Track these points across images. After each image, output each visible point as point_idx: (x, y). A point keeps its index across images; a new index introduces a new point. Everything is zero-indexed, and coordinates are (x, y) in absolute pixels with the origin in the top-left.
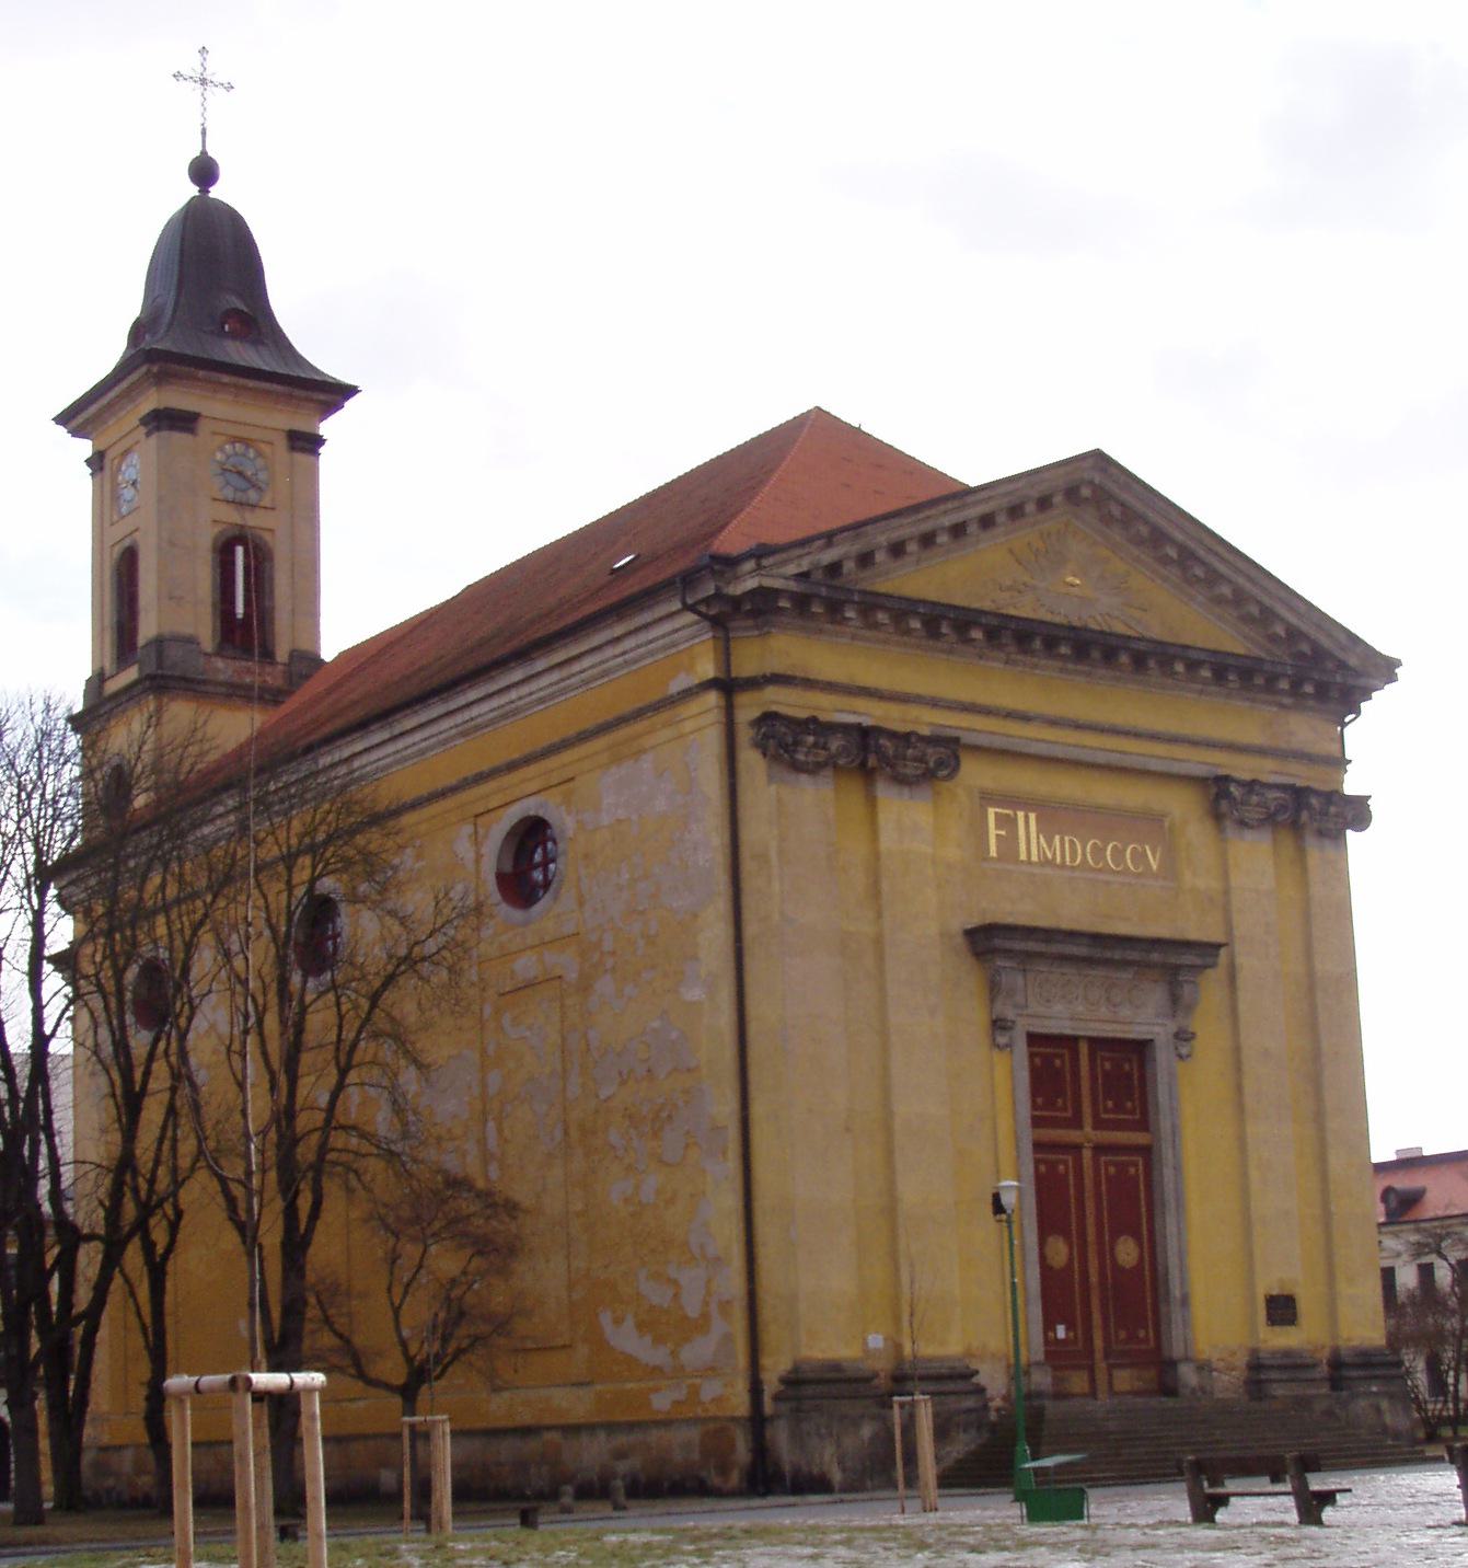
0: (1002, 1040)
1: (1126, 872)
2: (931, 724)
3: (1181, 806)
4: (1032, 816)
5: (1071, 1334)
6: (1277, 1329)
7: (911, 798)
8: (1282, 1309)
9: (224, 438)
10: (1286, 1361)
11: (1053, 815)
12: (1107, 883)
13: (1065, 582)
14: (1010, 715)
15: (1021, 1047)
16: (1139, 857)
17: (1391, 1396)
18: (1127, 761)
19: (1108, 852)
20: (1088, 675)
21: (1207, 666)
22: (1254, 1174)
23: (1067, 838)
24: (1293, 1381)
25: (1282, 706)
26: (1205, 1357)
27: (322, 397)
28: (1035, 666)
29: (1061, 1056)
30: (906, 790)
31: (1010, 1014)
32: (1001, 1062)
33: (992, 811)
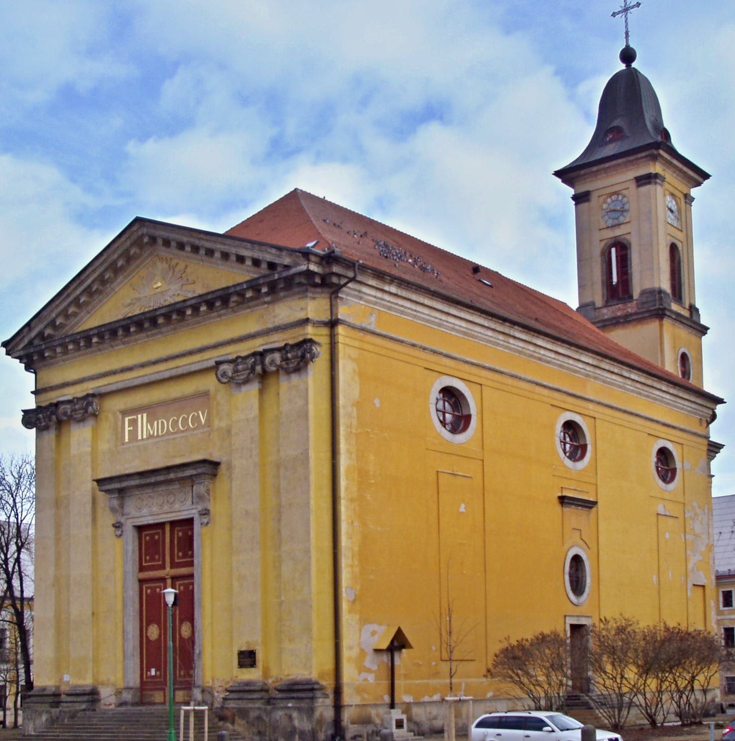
0: (119, 533)
1: (189, 429)
2: (92, 389)
3: (209, 382)
4: (145, 415)
5: (158, 673)
6: (244, 670)
7: (84, 426)
8: (247, 658)
9: (604, 197)
10: (247, 688)
11: (152, 410)
12: (174, 439)
13: (153, 288)
14: (123, 370)
15: (130, 535)
16: (196, 419)
17: (299, 710)
18: (180, 371)
19: (190, 421)
20: (161, 333)
21: (203, 304)
22: (236, 584)
23: (160, 421)
24: (239, 699)
25: (266, 303)
26: (210, 684)
27: (643, 154)
28: (136, 340)
29: (157, 534)
30: (82, 424)
31: (123, 520)
32: (118, 543)
33: (127, 419)
